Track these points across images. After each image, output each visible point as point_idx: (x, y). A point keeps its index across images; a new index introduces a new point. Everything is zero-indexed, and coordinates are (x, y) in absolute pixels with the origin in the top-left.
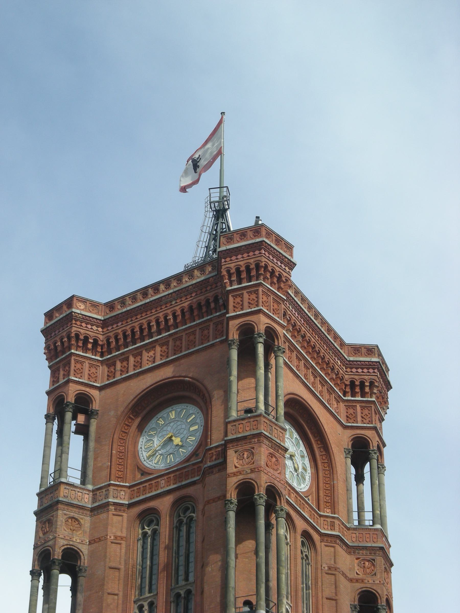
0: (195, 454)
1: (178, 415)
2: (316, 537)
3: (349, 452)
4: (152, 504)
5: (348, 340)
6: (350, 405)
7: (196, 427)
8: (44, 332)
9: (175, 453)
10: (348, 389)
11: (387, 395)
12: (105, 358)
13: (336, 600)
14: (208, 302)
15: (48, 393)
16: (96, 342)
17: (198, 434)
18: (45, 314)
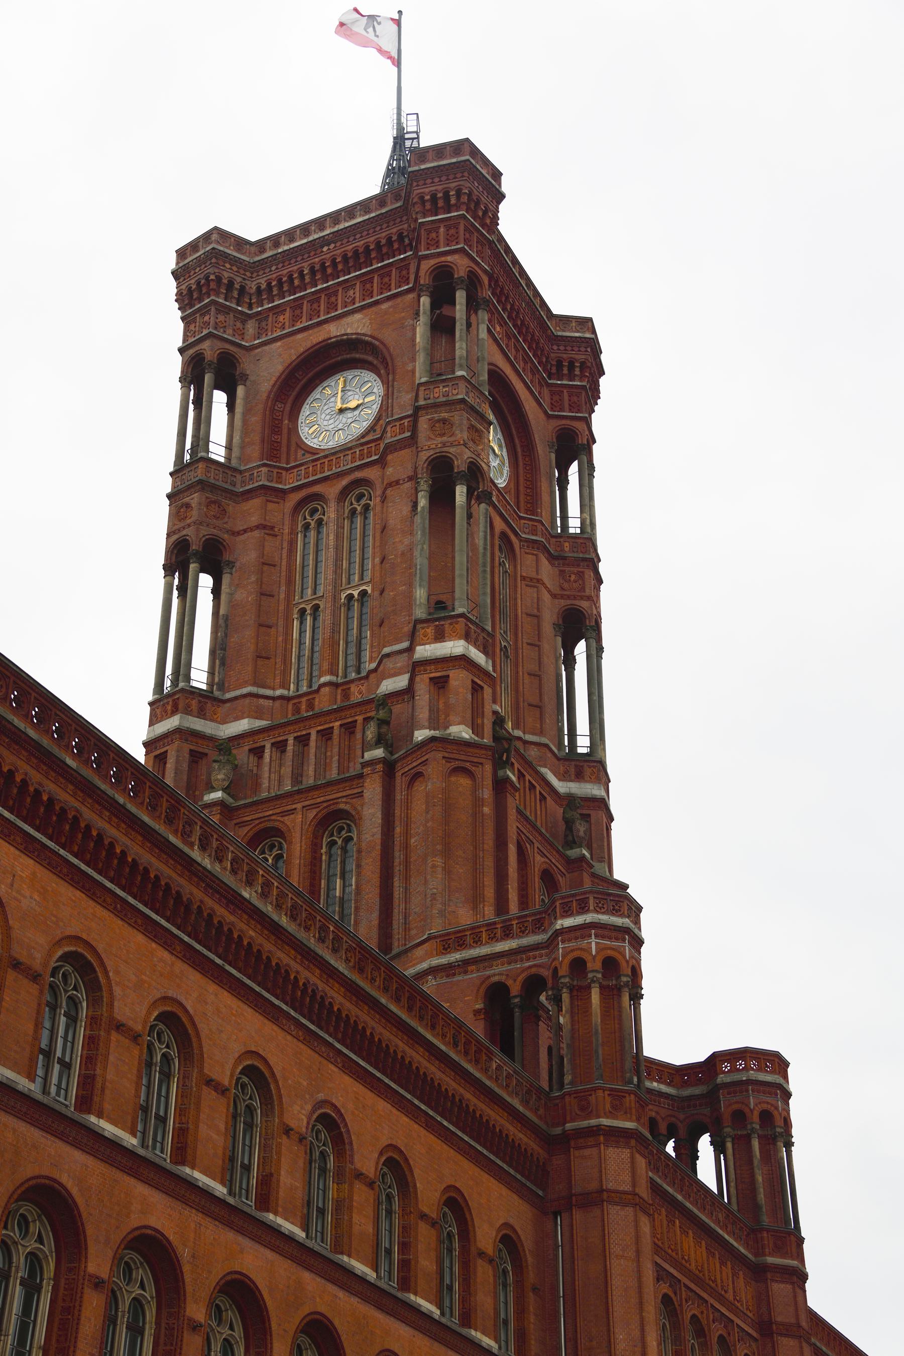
0: (371, 429)
3: (553, 446)
4: (317, 489)
5: (556, 310)
6: (556, 392)
7: (373, 398)
8: (175, 274)
9: (346, 428)
10: (554, 370)
11: (598, 382)
12: (254, 311)
13: (537, 617)
14: (389, 240)
15: (181, 351)
16: (242, 290)
17: (374, 407)
18: (177, 251)
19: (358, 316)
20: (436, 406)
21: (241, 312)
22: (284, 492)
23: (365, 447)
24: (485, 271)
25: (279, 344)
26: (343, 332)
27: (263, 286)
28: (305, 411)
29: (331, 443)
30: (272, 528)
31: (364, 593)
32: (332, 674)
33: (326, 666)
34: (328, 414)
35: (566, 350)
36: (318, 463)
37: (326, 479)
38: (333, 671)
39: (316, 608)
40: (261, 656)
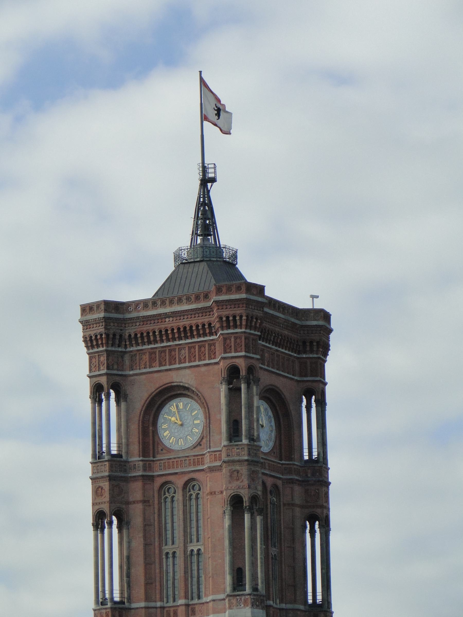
0: (199, 444)
1: (185, 406)
2: (279, 483)
17: (200, 427)
19: (188, 371)
20: (233, 461)
23: (196, 458)
24: (258, 359)
25: (143, 377)
26: (180, 381)
27: (133, 336)
28: (161, 420)
31: (199, 550)
33: (182, 594)
34: (175, 429)
35: (308, 333)
36: (171, 461)
37: (176, 473)
39: (174, 553)
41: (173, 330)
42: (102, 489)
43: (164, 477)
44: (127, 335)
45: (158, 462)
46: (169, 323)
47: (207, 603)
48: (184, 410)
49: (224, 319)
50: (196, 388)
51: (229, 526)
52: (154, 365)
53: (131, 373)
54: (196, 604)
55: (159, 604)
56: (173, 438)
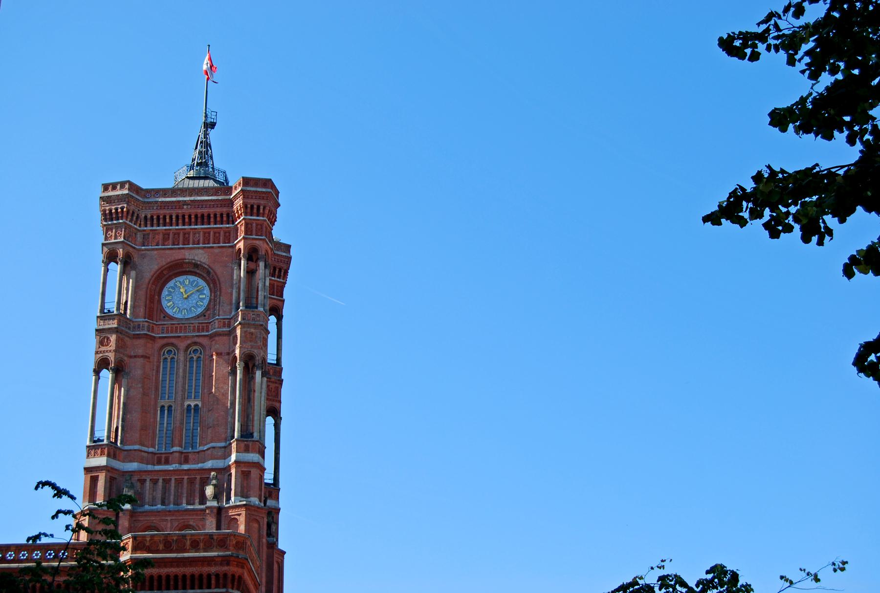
0: (203, 315)
1: (191, 283)
7: (204, 296)
9: (188, 309)
17: (205, 301)
19: (201, 251)
21: (136, 229)
22: (153, 339)
25: (155, 252)
26: (192, 258)
27: (149, 216)
29: (180, 315)
30: (149, 358)
31: (196, 406)
32: (180, 447)
36: (174, 326)
37: (179, 337)
38: (181, 446)
39: (170, 407)
40: (144, 428)
41: (190, 216)
42: (107, 339)
43: (166, 339)
44: (143, 216)
45: (161, 326)
46: (186, 210)
47: (204, 451)
48: (190, 285)
49: (249, 206)
50: (208, 265)
51: (240, 379)
52: (166, 244)
53: (143, 248)
54: (190, 453)
55: (151, 450)
56: (176, 308)
